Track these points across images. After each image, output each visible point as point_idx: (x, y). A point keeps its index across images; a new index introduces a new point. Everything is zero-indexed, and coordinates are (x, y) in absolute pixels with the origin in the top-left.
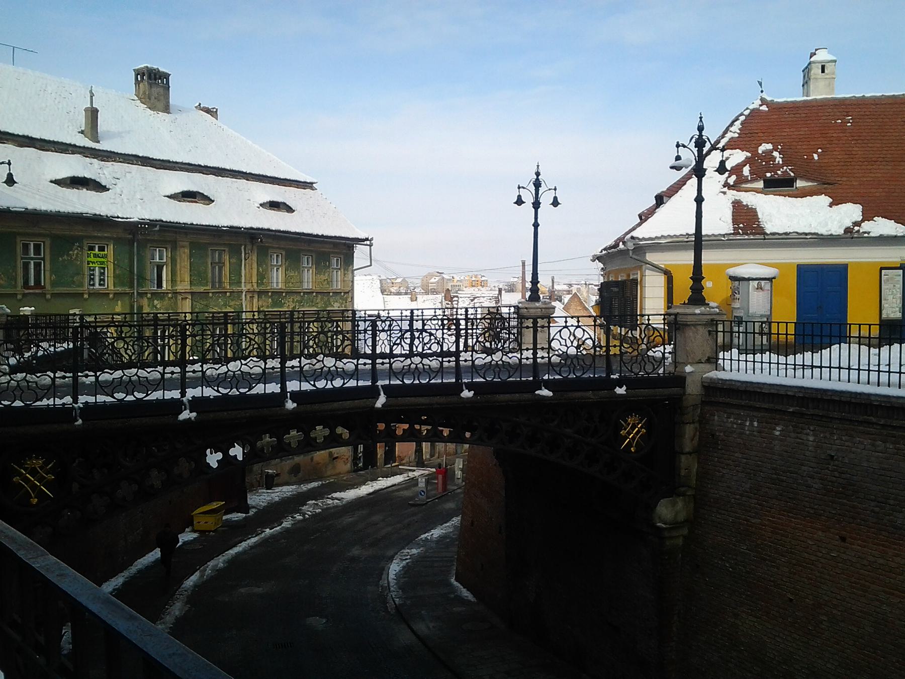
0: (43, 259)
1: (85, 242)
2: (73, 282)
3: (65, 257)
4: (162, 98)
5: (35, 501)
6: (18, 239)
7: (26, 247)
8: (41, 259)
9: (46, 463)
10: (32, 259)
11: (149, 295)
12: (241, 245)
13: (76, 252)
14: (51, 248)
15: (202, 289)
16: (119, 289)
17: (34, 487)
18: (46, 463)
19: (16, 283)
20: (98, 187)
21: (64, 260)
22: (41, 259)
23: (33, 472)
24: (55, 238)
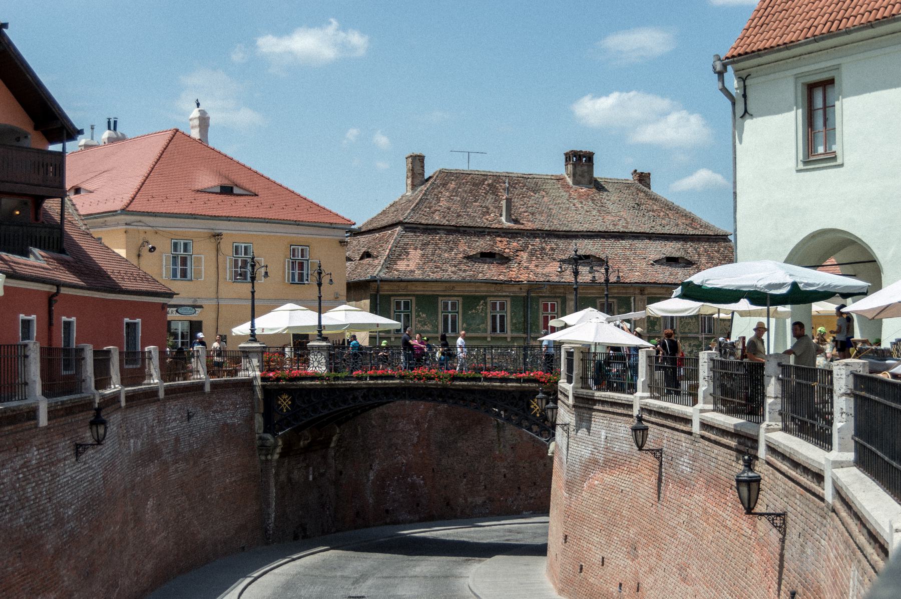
0: (458, 312)
2: (479, 329)
4: (586, 174)
5: (285, 411)
6: (440, 299)
9: (289, 397)
10: (450, 312)
12: (630, 297)
13: (481, 307)
16: (515, 335)
17: (285, 406)
18: (289, 397)
19: (438, 328)
20: (504, 260)
21: (473, 313)
23: (285, 400)
24: (465, 298)
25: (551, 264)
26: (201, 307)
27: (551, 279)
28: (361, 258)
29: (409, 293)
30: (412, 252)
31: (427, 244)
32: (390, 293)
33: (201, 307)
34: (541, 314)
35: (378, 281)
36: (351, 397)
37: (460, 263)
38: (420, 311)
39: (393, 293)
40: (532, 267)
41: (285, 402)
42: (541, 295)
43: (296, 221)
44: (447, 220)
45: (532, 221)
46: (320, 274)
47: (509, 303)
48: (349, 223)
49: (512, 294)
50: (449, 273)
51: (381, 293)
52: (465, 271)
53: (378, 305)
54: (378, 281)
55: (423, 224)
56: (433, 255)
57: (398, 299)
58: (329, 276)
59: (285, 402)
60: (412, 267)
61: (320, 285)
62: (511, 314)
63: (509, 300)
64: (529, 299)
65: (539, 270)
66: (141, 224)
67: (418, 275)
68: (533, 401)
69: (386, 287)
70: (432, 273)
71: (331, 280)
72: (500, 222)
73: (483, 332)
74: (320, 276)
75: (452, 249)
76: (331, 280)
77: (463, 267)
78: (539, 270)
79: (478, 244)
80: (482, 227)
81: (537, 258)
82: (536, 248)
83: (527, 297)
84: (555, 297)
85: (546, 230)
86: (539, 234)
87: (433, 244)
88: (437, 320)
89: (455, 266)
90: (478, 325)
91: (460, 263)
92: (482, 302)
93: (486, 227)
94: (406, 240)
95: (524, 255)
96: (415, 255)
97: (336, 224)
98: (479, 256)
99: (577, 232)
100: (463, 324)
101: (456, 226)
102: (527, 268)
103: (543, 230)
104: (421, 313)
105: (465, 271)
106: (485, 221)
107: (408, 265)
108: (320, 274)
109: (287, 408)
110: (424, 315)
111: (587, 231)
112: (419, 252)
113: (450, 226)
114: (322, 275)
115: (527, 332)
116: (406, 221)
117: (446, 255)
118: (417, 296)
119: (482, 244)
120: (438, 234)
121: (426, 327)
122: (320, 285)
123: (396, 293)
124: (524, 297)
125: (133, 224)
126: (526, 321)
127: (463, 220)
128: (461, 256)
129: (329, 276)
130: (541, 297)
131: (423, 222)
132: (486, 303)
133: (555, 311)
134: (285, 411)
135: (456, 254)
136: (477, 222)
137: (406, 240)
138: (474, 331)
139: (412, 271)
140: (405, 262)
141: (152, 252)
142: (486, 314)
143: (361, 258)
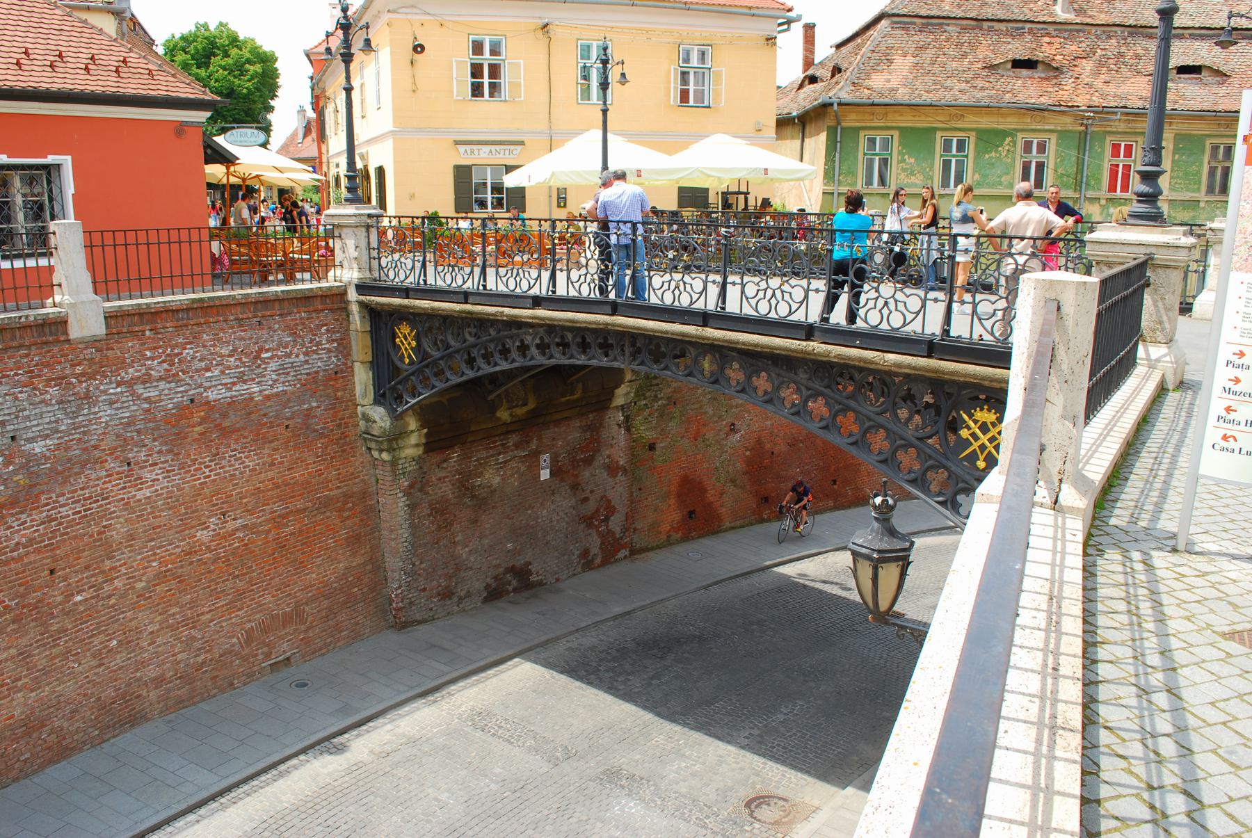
0: (967, 156)
1: (1020, 135)
2: (1001, 183)
3: (993, 154)
5: (407, 361)
6: (939, 134)
7: (872, 141)
8: (963, 156)
9: (412, 331)
11: (1103, 202)
14: (976, 145)
15: (1186, 196)
17: (406, 349)
18: (412, 331)
20: (1054, 70)
22: (963, 156)
25: (1132, 80)
26: (522, 143)
27: (1129, 104)
28: (833, 76)
29: (889, 124)
30: (898, 59)
31: (925, 47)
32: (858, 125)
33: (522, 143)
34: (1106, 160)
35: (835, 105)
36: (518, 343)
37: (977, 76)
38: (904, 154)
39: (864, 125)
40: (1098, 84)
41: (406, 339)
42: (1108, 129)
43: (686, 3)
44: (963, 11)
45: (1107, 12)
46: (605, 62)
47: (1054, 141)
48: (782, 7)
49: (1059, 128)
50: (956, 92)
51: (844, 124)
52: (982, 89)
53: (838, 144)
54: (835, 105)
55: (921, 17)
56: (933, 63)
57: (871, 133)
58: (620, 65)
59: (406, 339)
60: (894, 84)
61: (604, 85)
62: (1056, 159)
63: (1054, 137)
64: (1089, 137)
65: (1111, 89)
66: (415, 11)
67: (903, 96)
68: (971, 416)
69: (853, 116)
70: (927, 92)
71: (623, 75)
72: (1051, 13)
73: (1006, 187)
74: (605, 68)
75: (965, 55)
76: (623, 75)
77: (980, 83)
78: (1111, 89)
79: (1010, 46)
80: (1020, 21)
81: (1109, 70)
82: (1109, 53)
83: (1086, 134)
84: (1135, 134)
85: (1130, 26)
86: (1116, 32)
87: (934, 46)
88: (931, 168)
89: (967, 82)
90: (1000, 177)
91: (977, 76)
92: (1008, 140)
93: (1026, 21)
94: (891, 41)
95: (1087, 66)
96: (903, 65)
97: (757, 8)
98: (1009, 65)
99: (1184, 28)
100: (974, 175)
101: (976, 20)
102: (1090, 86)
103: (1124, 26)
104: (906, 157)
105: (982, 89)
106: (1027, 12)
107: (889, 81)
108: (605, 62)
109: (410, 356)
110: (912, 160)
111: (1200, 28)
112: (910, 59)
113: (967, 19)
114: (609, 66)
115: (1080, 191)
116: (893, 12)
117: (954, 64)
118: (901, 130)
119: (1018, 48)
120: (945, 31)
121: (913, 178)
122: (604, 85)
123: (868, 125)
124: (1080, 133)
125: (400, 11)
126: (1080, 171)
127: (989, 10)
128: (979, 66)
129: (620, 65)
130: (1110, 133)
131: (923, 13)
132: (1015, 143)
133: (1131, 156)
134: (407, 361)
135: (971, 63)
136: (1013, 13)
137: (891, 41)
138: (993, 186)
139: (896, 90)
140: (886, 76)
141: (421, 52)
142: (1014, 159)
143: (833, 76)
